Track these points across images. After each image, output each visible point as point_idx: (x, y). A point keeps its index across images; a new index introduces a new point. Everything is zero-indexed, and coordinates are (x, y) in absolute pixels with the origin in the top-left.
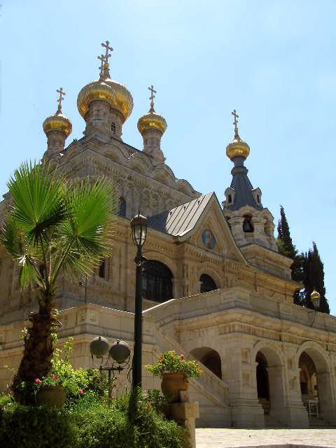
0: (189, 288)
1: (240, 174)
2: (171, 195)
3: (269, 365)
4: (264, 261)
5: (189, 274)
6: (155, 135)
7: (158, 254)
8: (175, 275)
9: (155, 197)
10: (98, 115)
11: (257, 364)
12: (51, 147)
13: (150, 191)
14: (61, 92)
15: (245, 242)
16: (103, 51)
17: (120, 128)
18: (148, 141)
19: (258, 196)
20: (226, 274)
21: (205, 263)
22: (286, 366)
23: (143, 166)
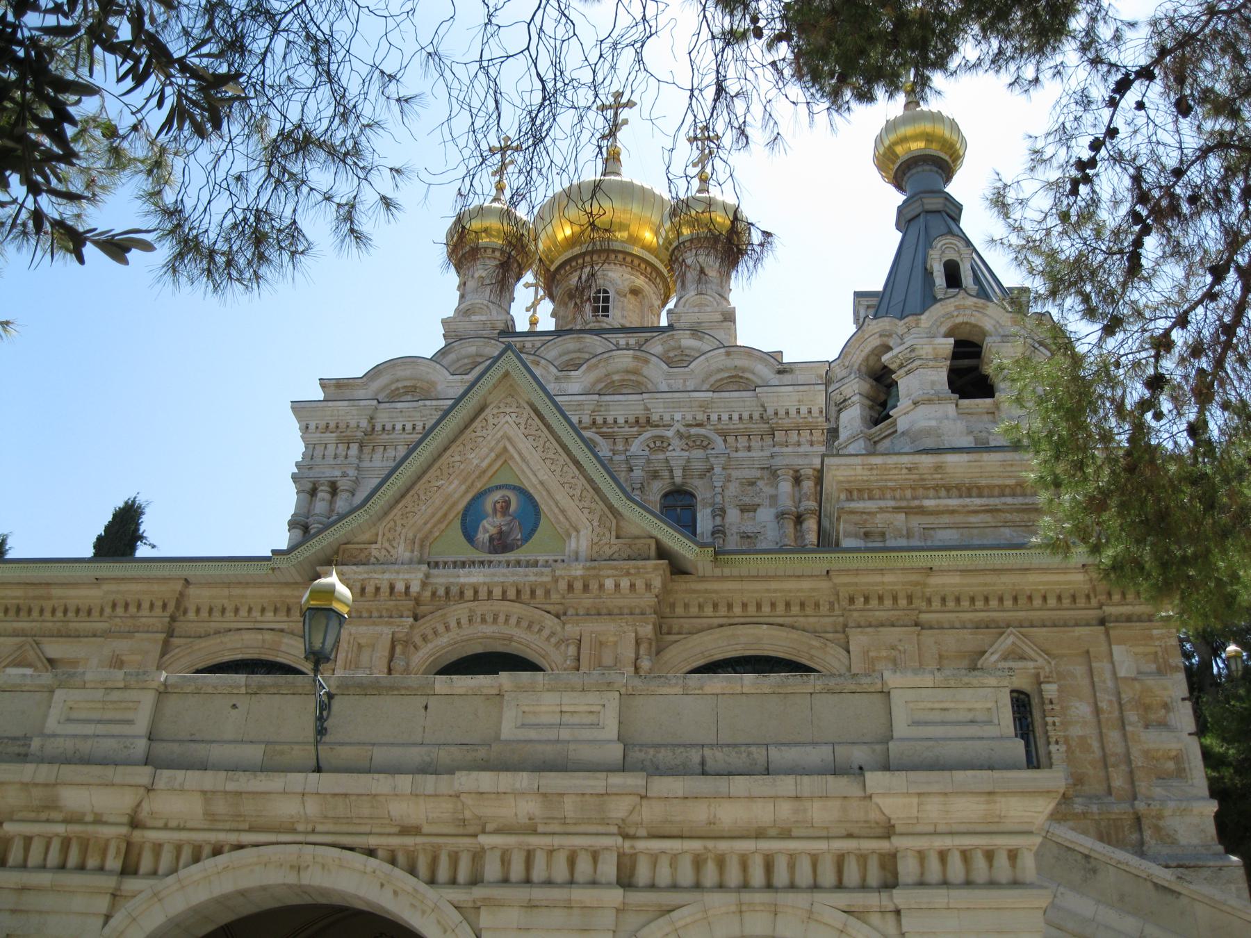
2: (655, 418)
4: (922, 511)
7: (248, 637)
20: (572, 630)
21: (459, 611)
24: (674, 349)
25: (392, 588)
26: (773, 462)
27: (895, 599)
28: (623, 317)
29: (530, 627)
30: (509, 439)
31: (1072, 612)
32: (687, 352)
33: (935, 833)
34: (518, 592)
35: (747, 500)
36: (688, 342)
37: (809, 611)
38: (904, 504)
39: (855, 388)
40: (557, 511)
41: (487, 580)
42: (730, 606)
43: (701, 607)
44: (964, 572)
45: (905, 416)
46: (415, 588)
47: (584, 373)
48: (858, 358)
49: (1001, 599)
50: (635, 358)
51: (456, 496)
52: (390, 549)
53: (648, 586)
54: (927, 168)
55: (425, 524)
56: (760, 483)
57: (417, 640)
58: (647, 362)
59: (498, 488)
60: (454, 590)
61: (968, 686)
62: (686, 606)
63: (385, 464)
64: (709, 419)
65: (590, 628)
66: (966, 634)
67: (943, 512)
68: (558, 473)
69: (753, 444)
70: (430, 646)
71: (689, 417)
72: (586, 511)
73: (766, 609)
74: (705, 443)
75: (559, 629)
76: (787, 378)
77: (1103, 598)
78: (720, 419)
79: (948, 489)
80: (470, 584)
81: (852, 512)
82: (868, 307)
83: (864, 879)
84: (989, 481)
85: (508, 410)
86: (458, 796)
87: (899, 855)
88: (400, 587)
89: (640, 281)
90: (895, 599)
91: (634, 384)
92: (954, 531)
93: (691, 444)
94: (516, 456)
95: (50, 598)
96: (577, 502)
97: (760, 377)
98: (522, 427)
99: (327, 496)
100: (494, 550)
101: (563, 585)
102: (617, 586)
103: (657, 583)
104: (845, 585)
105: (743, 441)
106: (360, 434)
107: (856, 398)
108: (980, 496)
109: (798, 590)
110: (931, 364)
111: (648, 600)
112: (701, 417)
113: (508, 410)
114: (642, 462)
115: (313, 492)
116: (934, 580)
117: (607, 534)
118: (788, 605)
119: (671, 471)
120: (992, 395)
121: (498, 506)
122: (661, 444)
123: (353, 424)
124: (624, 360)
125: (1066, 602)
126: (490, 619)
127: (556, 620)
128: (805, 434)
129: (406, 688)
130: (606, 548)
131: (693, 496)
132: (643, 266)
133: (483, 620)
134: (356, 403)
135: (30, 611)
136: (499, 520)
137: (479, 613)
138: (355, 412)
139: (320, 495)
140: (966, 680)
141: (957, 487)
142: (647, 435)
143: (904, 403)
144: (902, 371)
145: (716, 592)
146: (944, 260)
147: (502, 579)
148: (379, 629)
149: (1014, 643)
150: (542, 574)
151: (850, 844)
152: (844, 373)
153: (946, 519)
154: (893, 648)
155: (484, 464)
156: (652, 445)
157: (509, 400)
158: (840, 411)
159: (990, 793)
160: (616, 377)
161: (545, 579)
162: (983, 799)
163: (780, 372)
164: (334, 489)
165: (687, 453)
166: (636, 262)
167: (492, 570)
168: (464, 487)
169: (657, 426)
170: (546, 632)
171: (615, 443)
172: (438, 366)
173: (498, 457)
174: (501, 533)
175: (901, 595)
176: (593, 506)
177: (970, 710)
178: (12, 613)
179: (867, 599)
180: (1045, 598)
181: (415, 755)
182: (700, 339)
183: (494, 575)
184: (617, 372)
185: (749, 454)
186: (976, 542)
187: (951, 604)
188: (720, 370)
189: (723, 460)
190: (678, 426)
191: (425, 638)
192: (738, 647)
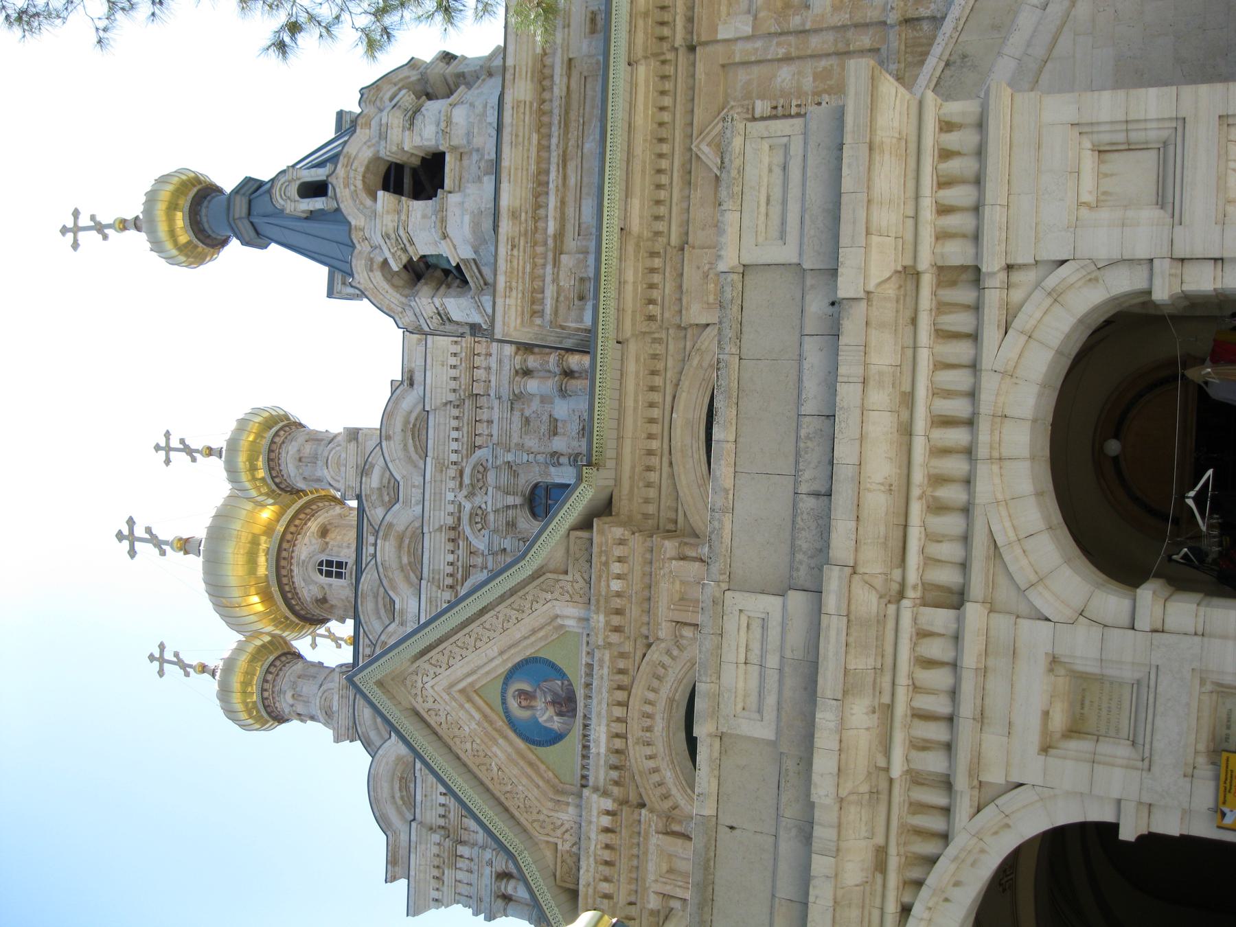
2: (450, 521)
4: (560, 236)
20: (665, 631)
21: (637, 755)
24: (381, 495)
25: (607, 830)
26: (505, 398)
27: (652, 270)
28: (348, 547)
29: (659, 678)
30: (452, 686)
31: (679, 80)
32: (385, 481)
33: (916, 218)
34: (620, 688)
35: (544, 428)
36: (374, 480)
37: (660, 366)
38: (550, 255)
39: (426, 302)
40: (533, 639)
41: (604, 722)
42: (650, 453)
43: (649, 485)
44: (628, 193)
45: (457, 250)
46: (609, 804)
47: (397, 593)
48: (394, 297)
49: (661, 156)
50: (385, 538)
51: (510, 750)
52: (563, 829)
53: (622, 542)
54: (204, 211)
55: (538, 787)
56: (527, 413)
57: (667, 805)
58: (390, 525)
59: (504, 702)
60: (614, 760)
61: (741, 171)
62: (647, 501)
64: (455, 463)
65: (664, 610)
66: (696, 196)
67: (563, 214)
68: (492, 634)
69: (485, 417)
70: (674, 791)
71: (452, 484)
72: (535, 606)
73: (656, 413)
74: (481, 469)
75: (663, 645)
76: (418, 377)
77: (665, 46)
78: (456, 452)
79: (537, 206)
80: (608, 742)
81: (556, 312)
82: (344, 283)
83: (967, 307)
84: (533, 161)
85: (419, 685)
86: (841, 800)
87: (940, 264)
88: (606, 821)
89: (313, 526)
90: (652, 270)
91: (413, 541)
92: (584, 202)
93: (481, 484)
94: (470, 680)
96: (525, 615)
97: (415, 406)
98: (438, 670)
99: (512, 883)
100: (573, 712)
101: (614, 638)
102: (619, 577)
103: (618, 532)
104: (633, 325)
105: (482, 428)
106: (448, 843)
107: (437, 301)
108: (548, 172)
109: (637, 375)
110: (403, 217)
111: (637, 543)
112: (452, 472)
113: (419, 685)
114: (496, 538)
115: (507, 898)
116: (635, 226)
117: (562, 584)
118: (652, 389)
119: (508, 507)
120: (442, 155)
121: (524, 703)
122: (479, 517)
123: (435, 850)
124: (387, 550)
125: (668, 86)
126: (648, 722)
127: (653, 648)
128: (478, 361)
129: (707, 848)
130: (577, 586)
131: (536, 486)
132: (297, 522)
133: (649, 729)
134: (413, 845)
136: (539, 704)
137: (641, 733)
138: (423, 847)
139: (510, 891)
140: (734, 173)
141: (537, 196)
142: (468, 530)
143: (444, 249)
144: (410, 249)
145: (633, 468)
146: (297, 198)
147: (604, 706)
148: (652, 848)
149: (709, 145)
150: (601, 661)
151: (924, 321)
152: (410, 313)
153: (570, 211)
154: (706, 276)
155: (477, 716)
156: (479, 526)
157: (408, 682)
158: (450, 320)
159: (871, 149)
160: (405, 560)
161: (607, 658)
162: (877, 157)
163: (411, 384)
165: (490, 489)
166: (292, 529)
167: (594, 716)
168: (501, 741)
169: (459, 519)
171: (474, 566)
172: (380, 752)
173: (470, 700)
174: (553, 703)
175: (648, 263)
176: (530, 597)
177: (770, 171)
179: (651, 302)
180: (662, 109)
181: (788, 845)
182: (373, 466)
183: (599, 714)
184: (400, 557)
185: (496, 422)
186: (596, 179)
187: (662, 210)
189: (500, 451)
190: (461, 497)
191: (666, 797)
192: (695, 446)
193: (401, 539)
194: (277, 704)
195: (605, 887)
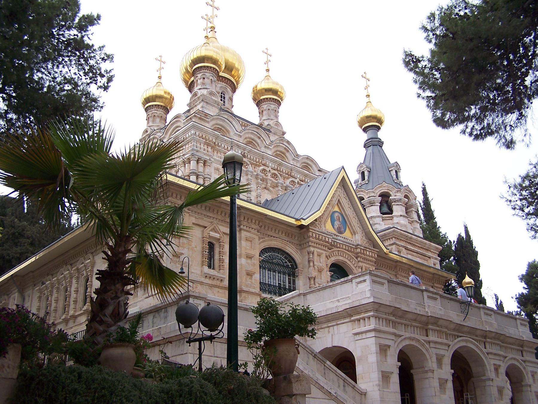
0: (316, 280)
1: (374, 144)
3: (415, 366)
5: (315, 263)
6: (273, 106)
8: (299, 266)
9: (274, 176)
10: (203, 84)
11: (399, 364)
12: (151, 124)
13: (268, 169)
14: (160, 61)
15: (384, 227)
16: (209, 11)
17: (231, 99)
18: (264, 113)
19: (396, 171)
22: (435, 366)
23: (259, 141)
47: (274, 147)
63: (218, 159)
88: (327, 239)
95: (220, 207)
135: (214, 211)
142: (291, 179)
160: (278, 153)
164: (205, 162)
170: (353, 263)
178: (208, 209)
188: (304, 163)
193: (283, 153)
194: (208, 71)
195: (314, 236)
